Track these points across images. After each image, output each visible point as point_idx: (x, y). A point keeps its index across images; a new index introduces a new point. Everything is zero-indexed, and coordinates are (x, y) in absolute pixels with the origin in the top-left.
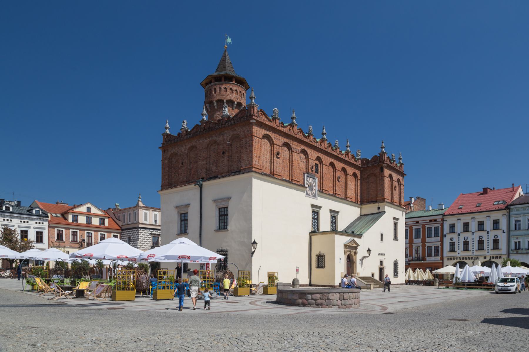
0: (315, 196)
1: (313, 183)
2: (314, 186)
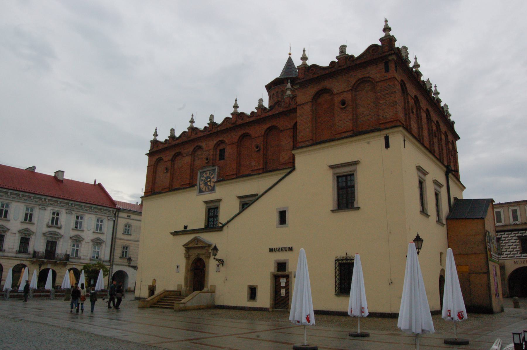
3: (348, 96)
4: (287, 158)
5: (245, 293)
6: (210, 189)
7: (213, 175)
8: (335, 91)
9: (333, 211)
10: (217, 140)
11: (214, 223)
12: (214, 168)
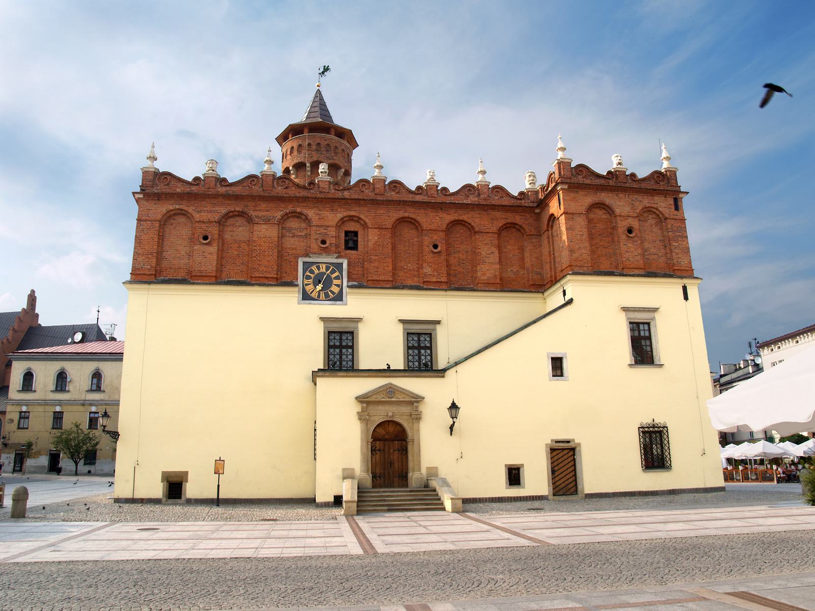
0: (339, 298)
1: (333, 272)
2: (337, 278)
3: (635, 224)
4: (490, 275)
5: (502, 476)
6: (331, 297)
7: (337, 274)
8: (618, 211)
9: (630, 365)
10: (345, 214)
11: (341, 357)
12: (339, 261)
